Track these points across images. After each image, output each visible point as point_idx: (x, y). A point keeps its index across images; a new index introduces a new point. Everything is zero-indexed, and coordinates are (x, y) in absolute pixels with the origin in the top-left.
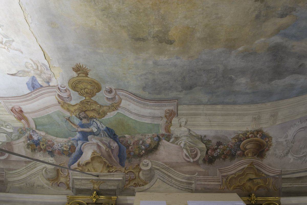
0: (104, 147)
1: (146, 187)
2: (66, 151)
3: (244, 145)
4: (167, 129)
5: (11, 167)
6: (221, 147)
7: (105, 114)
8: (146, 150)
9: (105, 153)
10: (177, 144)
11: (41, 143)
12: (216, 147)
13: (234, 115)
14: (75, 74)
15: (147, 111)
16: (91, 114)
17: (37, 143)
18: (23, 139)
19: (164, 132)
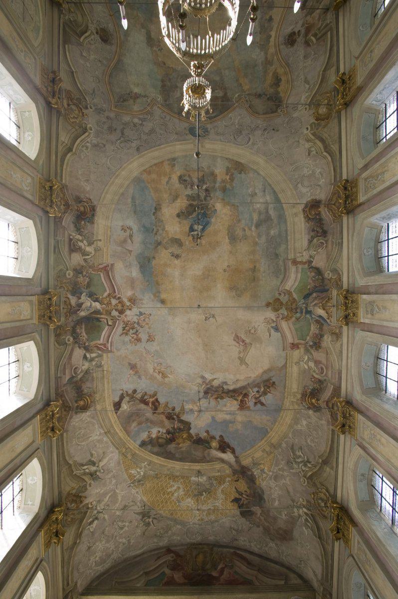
0: (316, 302)
1: (341, 273)
2: (320, 326)
3: (313, 216)
4: (304, 263)
5: (330, 365)
6: (315, 229)
7: (294, 299)
8: (319, 275)
9: (321, 301)
10: (315, 256)
11: (315, 341)
12: (316, 232)
13: (294, 228)
14: (270, 308)
15: (293, 276)
16: (294, 306)
17: (315, 344)
18: (312, 352)
19: (307, 265)
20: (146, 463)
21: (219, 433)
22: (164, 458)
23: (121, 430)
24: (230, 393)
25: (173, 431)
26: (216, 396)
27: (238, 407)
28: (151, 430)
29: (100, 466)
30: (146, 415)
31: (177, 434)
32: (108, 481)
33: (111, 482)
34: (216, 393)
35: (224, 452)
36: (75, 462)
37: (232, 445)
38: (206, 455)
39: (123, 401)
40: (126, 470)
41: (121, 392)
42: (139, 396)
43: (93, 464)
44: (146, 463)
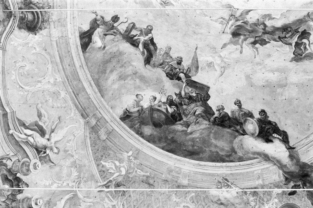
20: (130, 153)
21: (260, 107)
22: (163, 149)
23: (90, 83)
24: (277, 32)
25: (178, 100)
26: (252, 40)
27: (293, 56)
28: (142, 93)
29: (53, 140)
30: (134, 64)
31: (185, 107)
32: (65, 171)
33: (69, 175)
34: (253, 34)
35: (268, 141)
36: (13, 113)
37: (282, 127)
38: (235, 146)
39: (96, 32)
40: (97, 160)
41: (94, 16)
42: (122, 28)
43: (42, 132)
44: (130, 153)
